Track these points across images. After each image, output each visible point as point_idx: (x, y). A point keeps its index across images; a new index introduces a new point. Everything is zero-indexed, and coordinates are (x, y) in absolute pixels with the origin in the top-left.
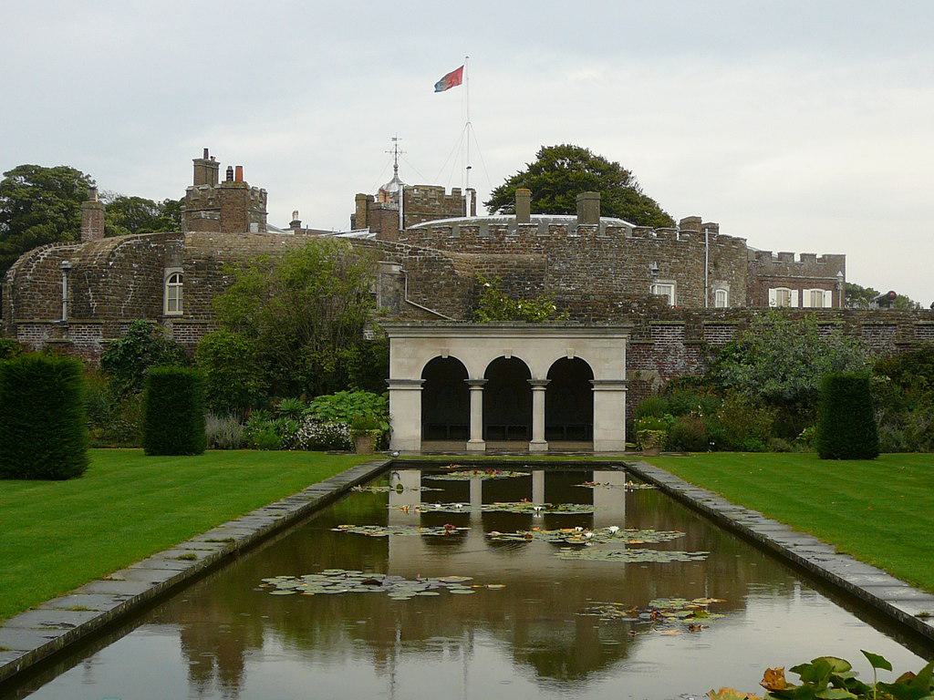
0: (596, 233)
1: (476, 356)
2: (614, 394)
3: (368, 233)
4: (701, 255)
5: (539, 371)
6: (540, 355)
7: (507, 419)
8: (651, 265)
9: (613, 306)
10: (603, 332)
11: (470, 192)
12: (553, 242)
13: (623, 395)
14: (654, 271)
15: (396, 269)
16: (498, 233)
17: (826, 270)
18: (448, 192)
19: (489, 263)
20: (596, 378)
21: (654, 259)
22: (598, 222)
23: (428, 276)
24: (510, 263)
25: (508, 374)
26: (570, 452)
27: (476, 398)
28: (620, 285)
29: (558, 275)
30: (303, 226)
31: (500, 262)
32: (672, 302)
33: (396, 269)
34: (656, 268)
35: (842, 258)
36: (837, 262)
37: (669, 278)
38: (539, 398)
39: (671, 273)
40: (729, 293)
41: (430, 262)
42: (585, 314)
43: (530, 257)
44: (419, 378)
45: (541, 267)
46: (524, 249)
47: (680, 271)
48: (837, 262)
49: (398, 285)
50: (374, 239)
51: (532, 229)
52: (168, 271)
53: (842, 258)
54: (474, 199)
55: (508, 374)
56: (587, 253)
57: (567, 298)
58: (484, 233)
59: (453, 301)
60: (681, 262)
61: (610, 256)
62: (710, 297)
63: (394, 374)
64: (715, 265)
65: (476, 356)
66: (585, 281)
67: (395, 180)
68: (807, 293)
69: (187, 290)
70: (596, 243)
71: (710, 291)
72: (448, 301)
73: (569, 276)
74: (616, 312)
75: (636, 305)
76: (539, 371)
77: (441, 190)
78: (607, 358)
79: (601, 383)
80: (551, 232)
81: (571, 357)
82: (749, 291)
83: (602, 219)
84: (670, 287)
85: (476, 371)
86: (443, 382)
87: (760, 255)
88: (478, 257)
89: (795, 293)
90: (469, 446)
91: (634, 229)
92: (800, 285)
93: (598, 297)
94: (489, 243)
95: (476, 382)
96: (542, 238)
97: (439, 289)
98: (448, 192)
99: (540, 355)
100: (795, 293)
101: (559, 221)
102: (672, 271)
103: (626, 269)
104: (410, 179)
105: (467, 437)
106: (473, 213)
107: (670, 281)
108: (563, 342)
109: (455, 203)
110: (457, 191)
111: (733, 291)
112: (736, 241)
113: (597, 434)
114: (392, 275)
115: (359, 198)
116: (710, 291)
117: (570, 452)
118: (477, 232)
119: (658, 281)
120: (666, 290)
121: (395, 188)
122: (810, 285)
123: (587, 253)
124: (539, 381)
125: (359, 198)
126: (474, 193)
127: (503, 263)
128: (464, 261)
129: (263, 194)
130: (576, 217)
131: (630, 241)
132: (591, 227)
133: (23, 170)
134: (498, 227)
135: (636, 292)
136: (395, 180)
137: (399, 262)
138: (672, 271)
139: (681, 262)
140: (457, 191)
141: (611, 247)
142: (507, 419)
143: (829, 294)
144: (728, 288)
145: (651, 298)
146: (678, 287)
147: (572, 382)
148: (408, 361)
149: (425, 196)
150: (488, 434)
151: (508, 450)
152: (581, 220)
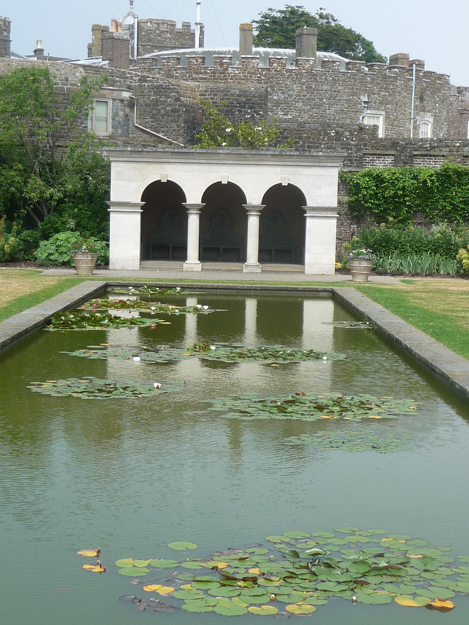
0: (312, 67)
1: (194, 181)
2: (326, 221)
3: (100, 60)
4: (408, 88)
5: (254, 196)
6: (255, 181)
7: (223, 244)
8: (362, 97)
9: (326, 134)
10: (317, 162)
11: (199, 27)
12: (272, 74)
13: (335, 221)
14: (365, 102)
15: (126, 95)
16: (221, 64)
18: (179, 26)
19: (214, 91)
20: (311, 202)
21: (365, 91)
22: (315, 57)
23: (156, 103)
24: (232, 91)
25: (224, 201)
26: (281, 276)
27: (193, 223)
28: (333, 115)
29: (277, 104)
30: (45, 54)
31: (223, 91)
32: (381, 134)
33: (126, 95)
34: (366, 100)
37: (378, 109)
40: (434, 124)
41: (159, 90)
42: (298, 143)
43: (252, 87)
44: (137, 199)
46: (246, 79)
47: (389, 103)
49: (127, 110)
50: (107, 67)
51: (254, 61)
54: (202, 33)
55: (224, 201)
56: (303, 84)
57: (284, 125)
58: (210, 66)
59: (178, 126)
60: (390, 95)
61: (325, 87)
62: (414, 128)
63: (114, 197)
64: (422, 99)
65: (194, 181)
66: (300, 111)
71: (415, 122)
72: (174, 125)
73: (287, 106)
74: (328, 138)
75: (347, 133)
76: (254, 196)
77: (173, 25)
78: (320, 186)
79: (314, 209)
80: (271, 64)
81: (285, 184)
83: (319, 53)
84: (427, 125)
85: (194, 196)
86: (162, 203)
90: (186, 265)
91: (348, 64)
93: (313, 126)
94: (214, 73)
95: (193, 206)
96: (263, 69)
97: (166, 114)
98: (179, 26)
99: (255, 181)
101: (279, 54)
102: (381, 103)
103: (339, 100)
104: (144, 16)
106: (201, 45)
107: (378, 112)
108: (278, 169)
110: (187, 26)
111: (437, 121)
112: (441, 77)
113: (308, 257)
114: (122, 101)
115: (96, 29)
116: (415, 122)
117: (281, 276)
118: (203, 62)
119: (369, 112)
120: (376, 121)
123: (303, 84)
124: (253, 207)
125: (96, 29)
127: (226, 92)
128: (193, 89)
130: (294, 51)
131: (344, 74)
132: (308, 61)
134: (223, 58)
135: (348, 121)
137: (129, 88)
138: (381, 103)
139: (390, 95)
140: (187, 26)
141: (326, 79)
142: (223, 244)
144: (431, 120)
145: (361, 129)
146: (387, 117)
148: (128, 183)
149: (157, 29)
150: (204, 256)
152: (299, 54)
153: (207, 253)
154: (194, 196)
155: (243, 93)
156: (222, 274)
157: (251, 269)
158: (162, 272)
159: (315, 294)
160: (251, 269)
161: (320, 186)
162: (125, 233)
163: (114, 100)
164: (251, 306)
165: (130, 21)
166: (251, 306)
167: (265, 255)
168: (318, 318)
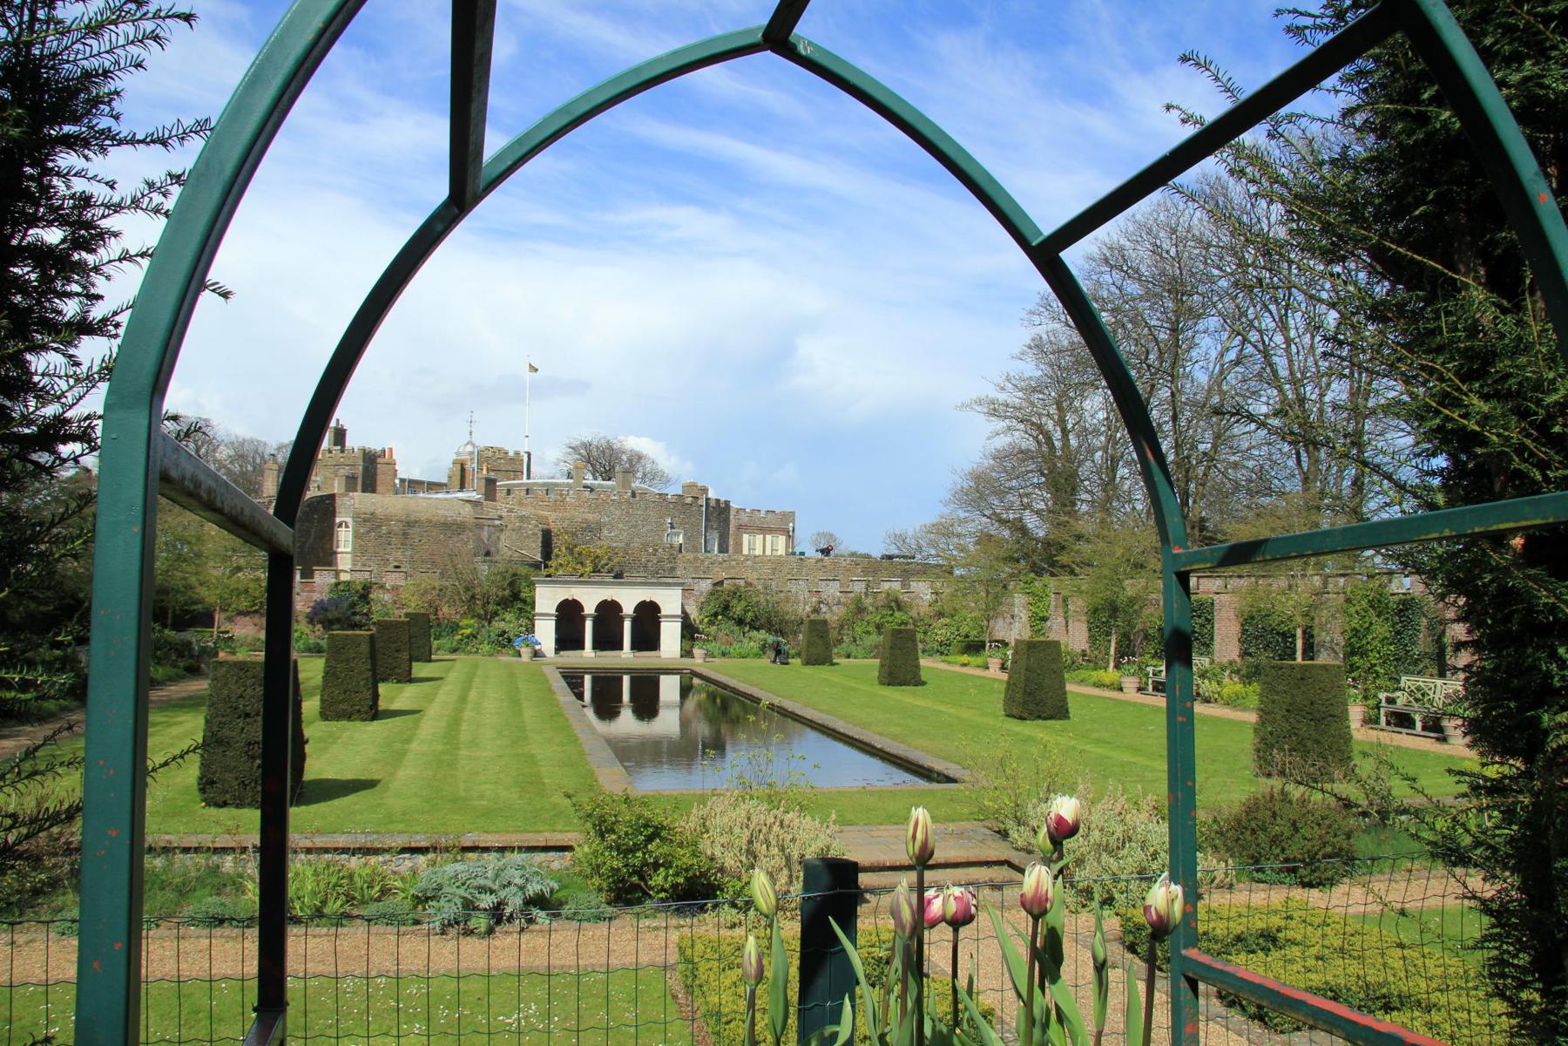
1: (590, 598)
5: (628, 608)
6: (629, 599)
7: (607, 639)
18: (511, 454)
19: (563, 519)
20: (663, 612)
25: (608, 611)
26: (645, 659)
36: (789, 516)
38: (627, 625)
44: (553, 611)
48: (789, 516)
52: (338, 520)
55: (608, 611)
63: (538, 610)
65: (590, 598)
68: (769, 537)
69: (356, 536)
76: (628, 608)
78: (670, 601)
85: (590, 608)
86: (569, 614)
87: (738, 511)
89: (759, 538)
92: (764, 530)
98: (511, 454)
99: (629, 599)
104: (483, 441)
105: (582, 647)
117: (645, 659)
122: (770, 530)
126: (529, 455)
127: (571, 520)
140: (517, 453)
142: (607, 639)
143: (782, 540)
147: (648, 615)
148: (547, 599)
151: (609, 659)
153: (598, 645)
155: (586, 521)
156: (609, 659)
157: (626, 655)
158: (571, 658)
159: (669, 671)
160: (626, 655)
162: (546, 633)
164: (626, 680)
165: (469, 448)
166: (626, 680)
167: (637, 645)
168: (669, 688)
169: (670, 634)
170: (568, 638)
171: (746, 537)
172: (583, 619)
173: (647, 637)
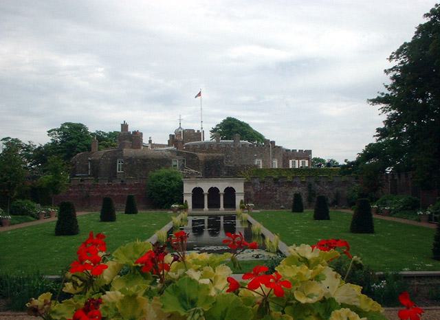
1: (206, 186)
5: (222, 191)
6: (222, 186)
7: (214, 204)
17: (306, 154)
25: (214, 192)
26: (230, 212)
30: (153, 143)
35: (311, 151)
36: (309, 152)
38: (222, 198)
39: (261, 157)
42: (233, 173)
44: (191, 192)
45: (223, 157)
48: (309, 152)
53: (311, 151)
55: (214, 192)
63: (185, 192)
65: (206, 186)
67: (180, 127)
68: (301, 161)
70: (239, 149)
76: (222, 191)
77: (194, 131)
78: (239, 188)
82: (284, 161)
85: (206, 191)
86: (197, 193)
88: (205, 155)
89: (297, 161)
92: (298, 159)
99: (222, 186)
100: (297, 161)
109: (198, 135)
110: (198, 131)
112: (279, 147)
115: (170, 135)
117: (230, 212)
121: (180, 130)
125: (170, 135)
129: (141, 134)
133: (66, 124)
136: (180, 127)
140: (198, 131)
142: (214, 204)
143: (307, 161)
146: (263, 161)
147: (230, 192)
148: (188, 189)
154: (206, 191)
161: (239, 188)
163: (179, 160)
169: (239, 199)
170: (198, 203)
171: (291, 161)
172: (203, 195)
173: (230, 203)
